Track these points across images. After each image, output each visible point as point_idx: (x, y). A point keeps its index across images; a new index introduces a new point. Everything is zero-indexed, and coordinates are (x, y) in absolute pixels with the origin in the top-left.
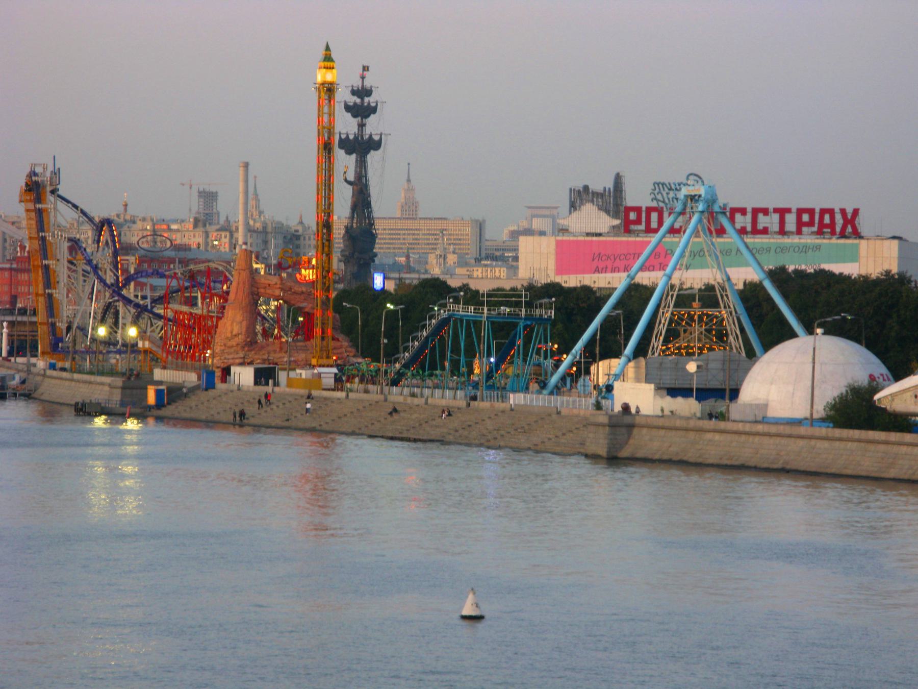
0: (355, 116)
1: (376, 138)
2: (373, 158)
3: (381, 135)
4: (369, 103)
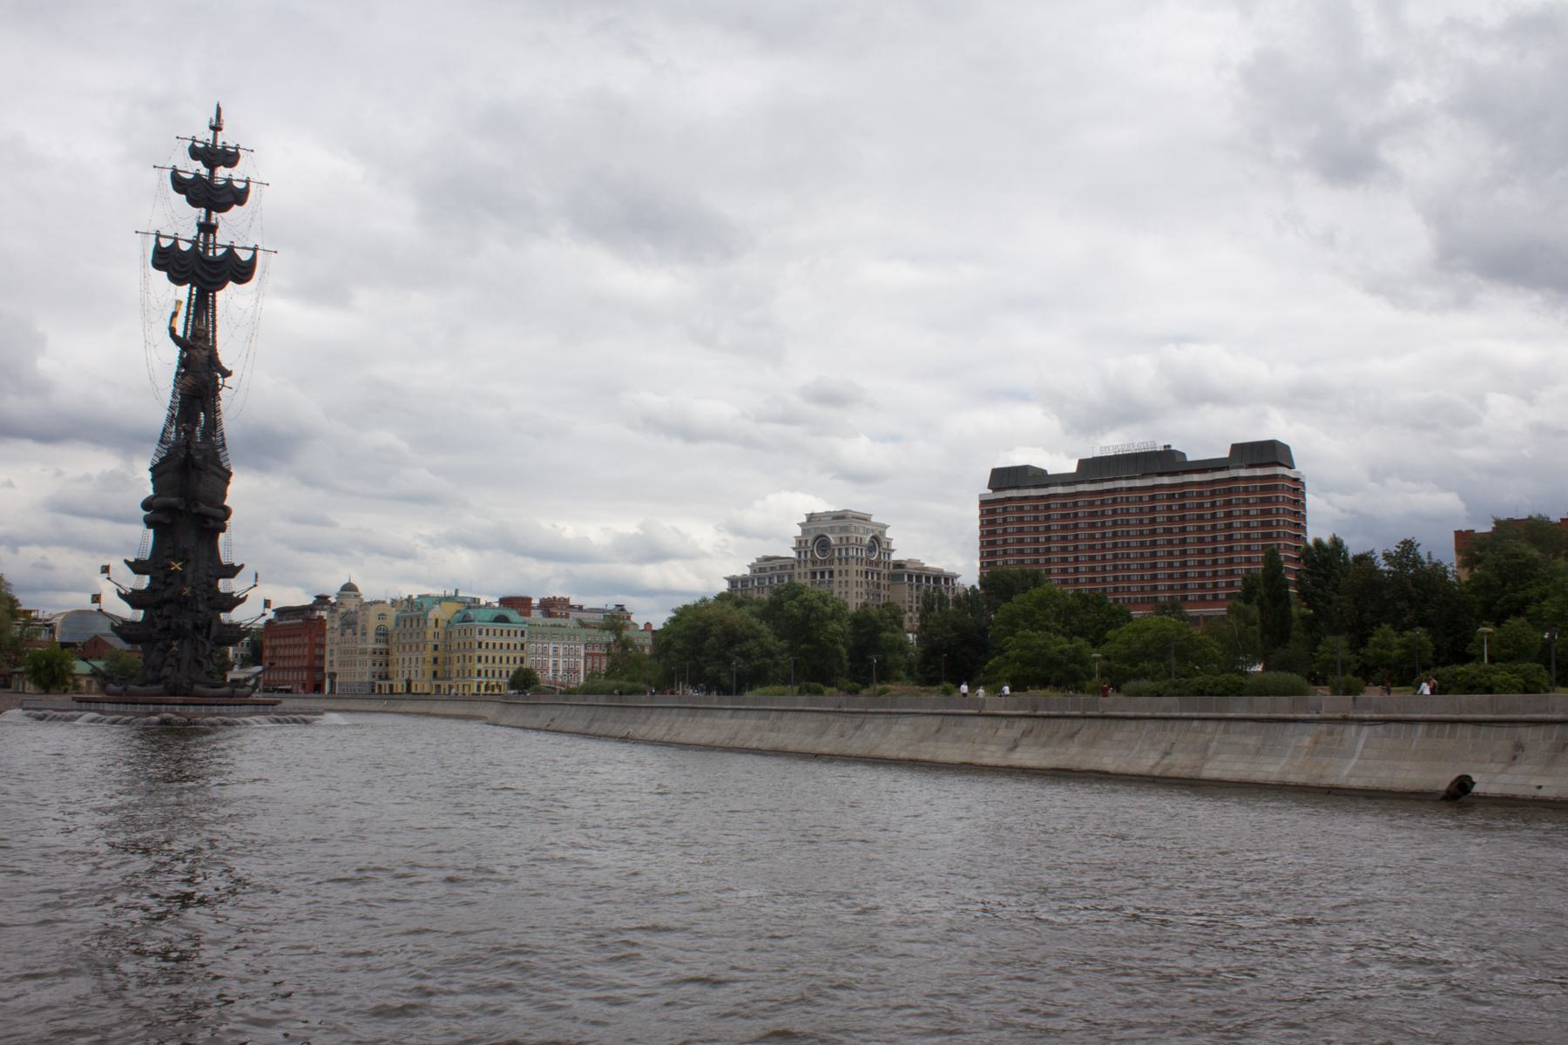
0: (194, 202)
1: (245, 256)
2: (229, 298)
3: (255, 250)
4: (229, 181)
